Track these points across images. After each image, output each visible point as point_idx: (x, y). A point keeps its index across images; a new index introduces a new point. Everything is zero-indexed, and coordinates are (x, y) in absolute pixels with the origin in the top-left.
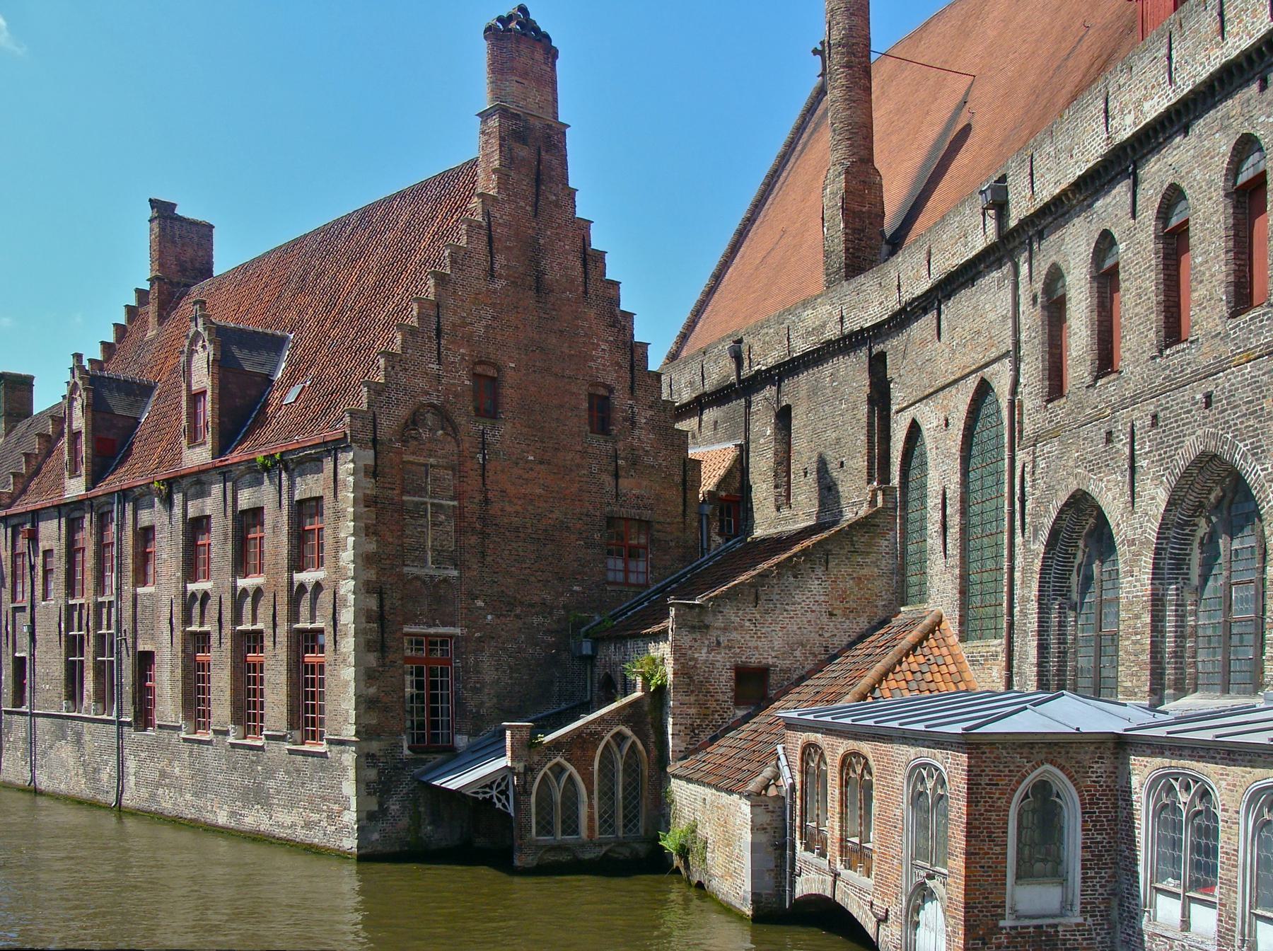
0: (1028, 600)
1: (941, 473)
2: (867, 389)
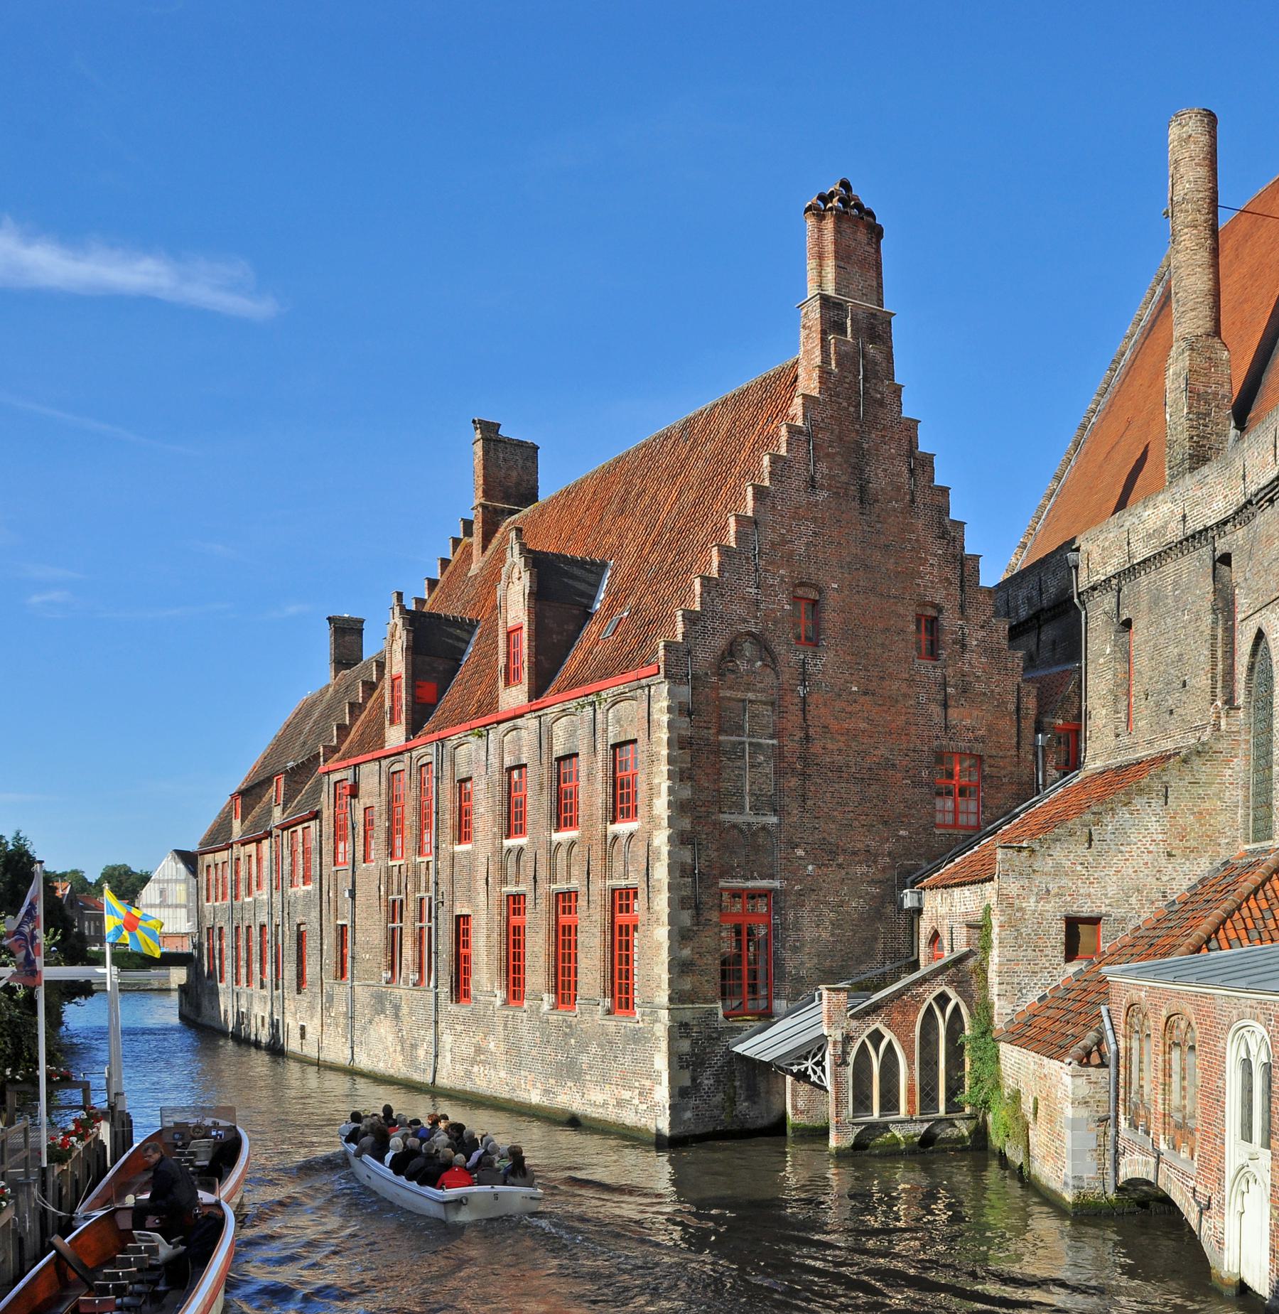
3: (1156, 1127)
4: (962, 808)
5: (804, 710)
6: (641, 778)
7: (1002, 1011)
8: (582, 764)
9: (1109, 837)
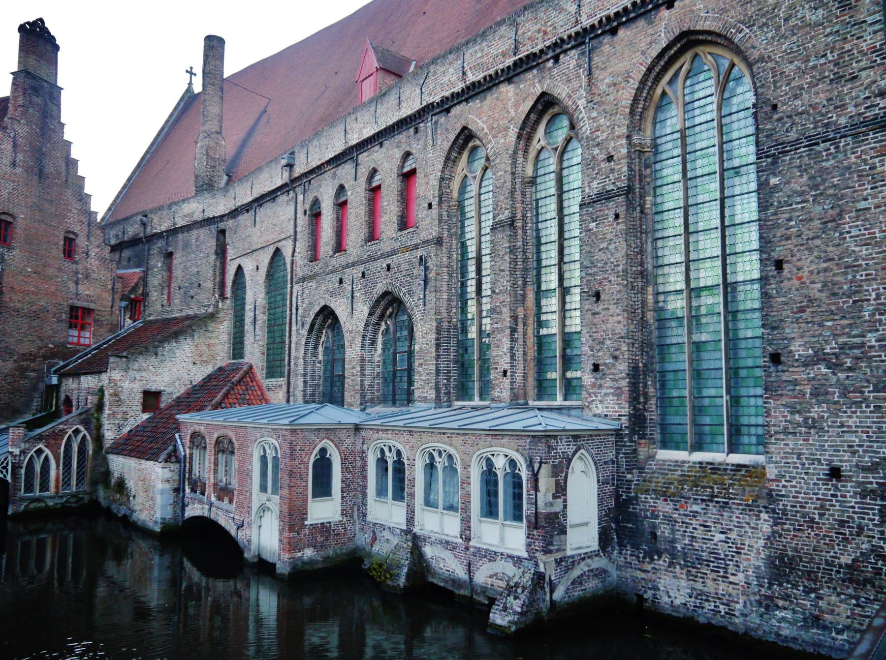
1: (255, 293)
2: (214, 247)
3: (209, 490)
7: (109, 435)
9: (166, 353)
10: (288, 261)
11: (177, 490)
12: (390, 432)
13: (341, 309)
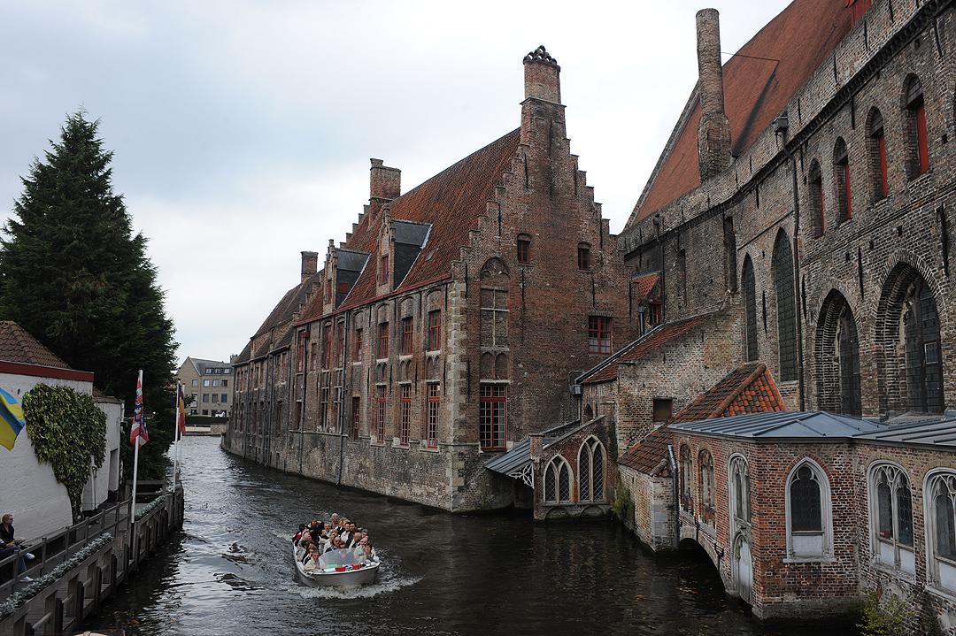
0: (810, 356)
1: (764, 283)
3: (696, 510)
4: (603, 343)
5: (523, 295)
6: (442, 328)
7: (622, 445)
8: (415, 322)
9: (674, 358)
10: (792, 242)
11: (670, 507)
12: (889, 450)
13: (850, 292)
